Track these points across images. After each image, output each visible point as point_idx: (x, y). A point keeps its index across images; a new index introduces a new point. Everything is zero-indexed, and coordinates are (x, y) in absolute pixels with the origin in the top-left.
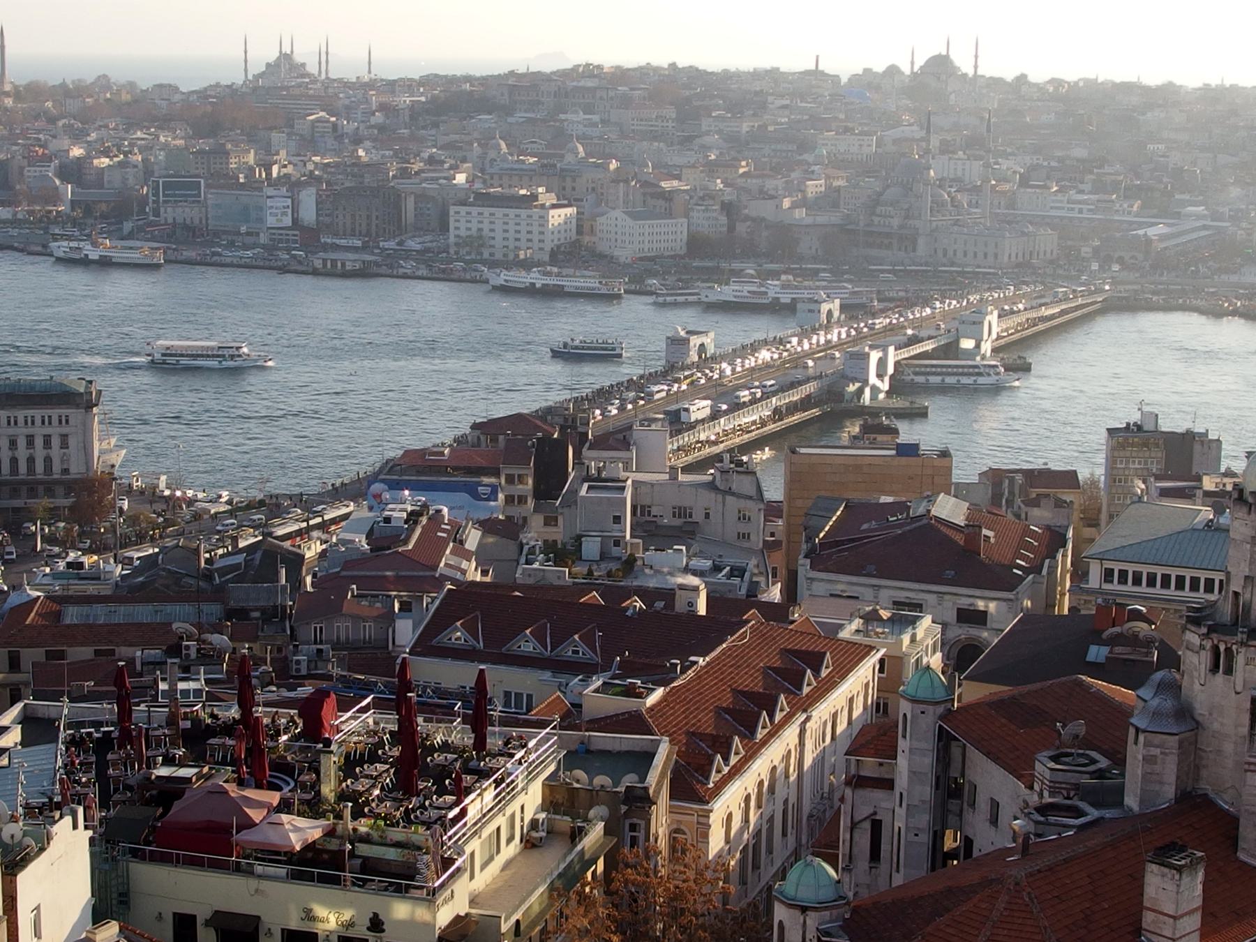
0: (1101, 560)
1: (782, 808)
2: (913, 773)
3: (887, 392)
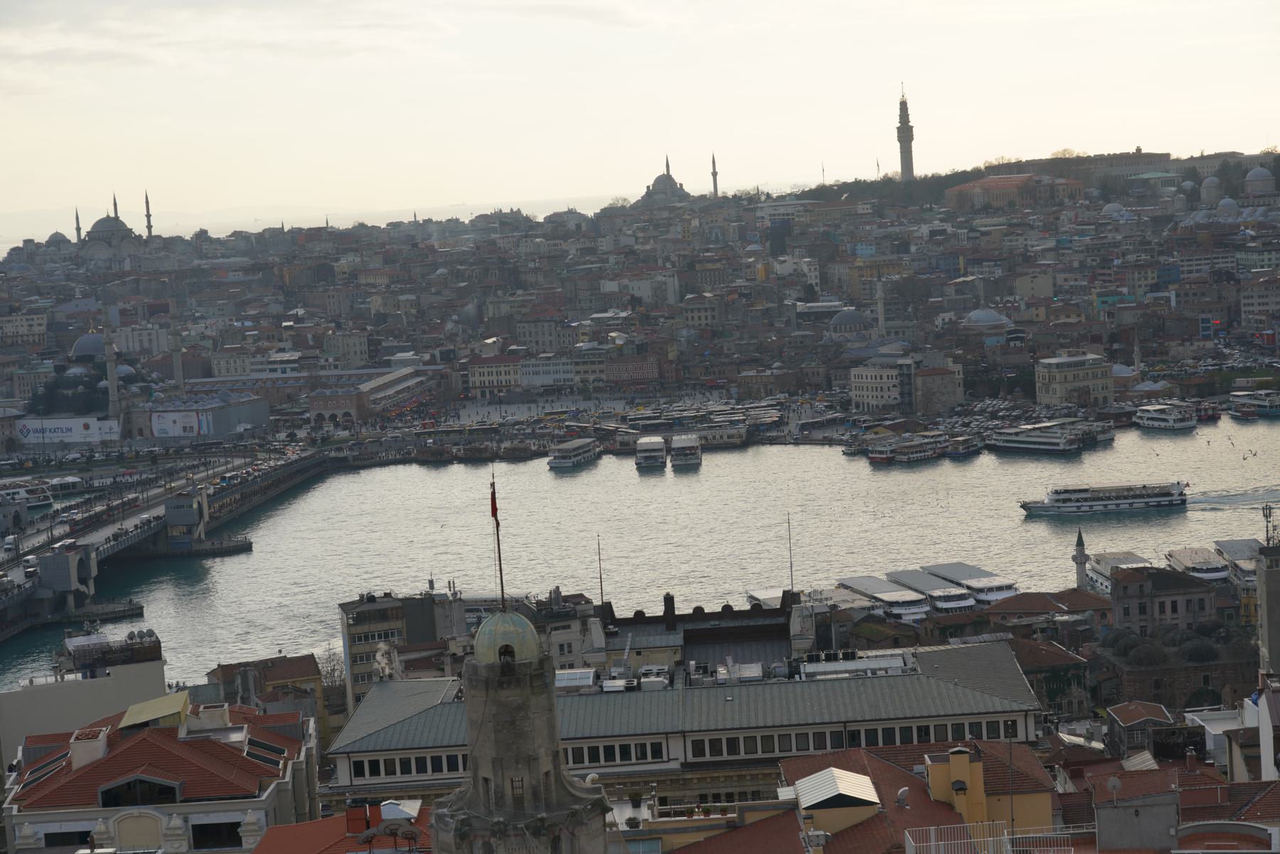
0: (348, 753)
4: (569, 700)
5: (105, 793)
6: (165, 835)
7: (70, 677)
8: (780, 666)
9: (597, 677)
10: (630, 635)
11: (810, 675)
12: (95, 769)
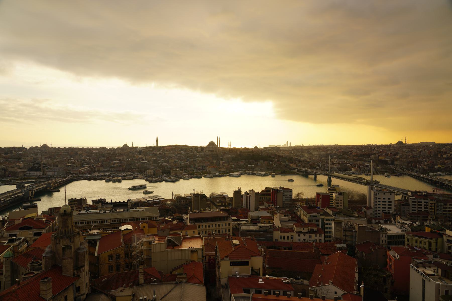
2: (6, 271)
3: (33, 197)
6: (29, 234)
8: (126, 210)
9: (100, 211)
10: (105, 205)
11: (130, 211)
12: (19, 224)
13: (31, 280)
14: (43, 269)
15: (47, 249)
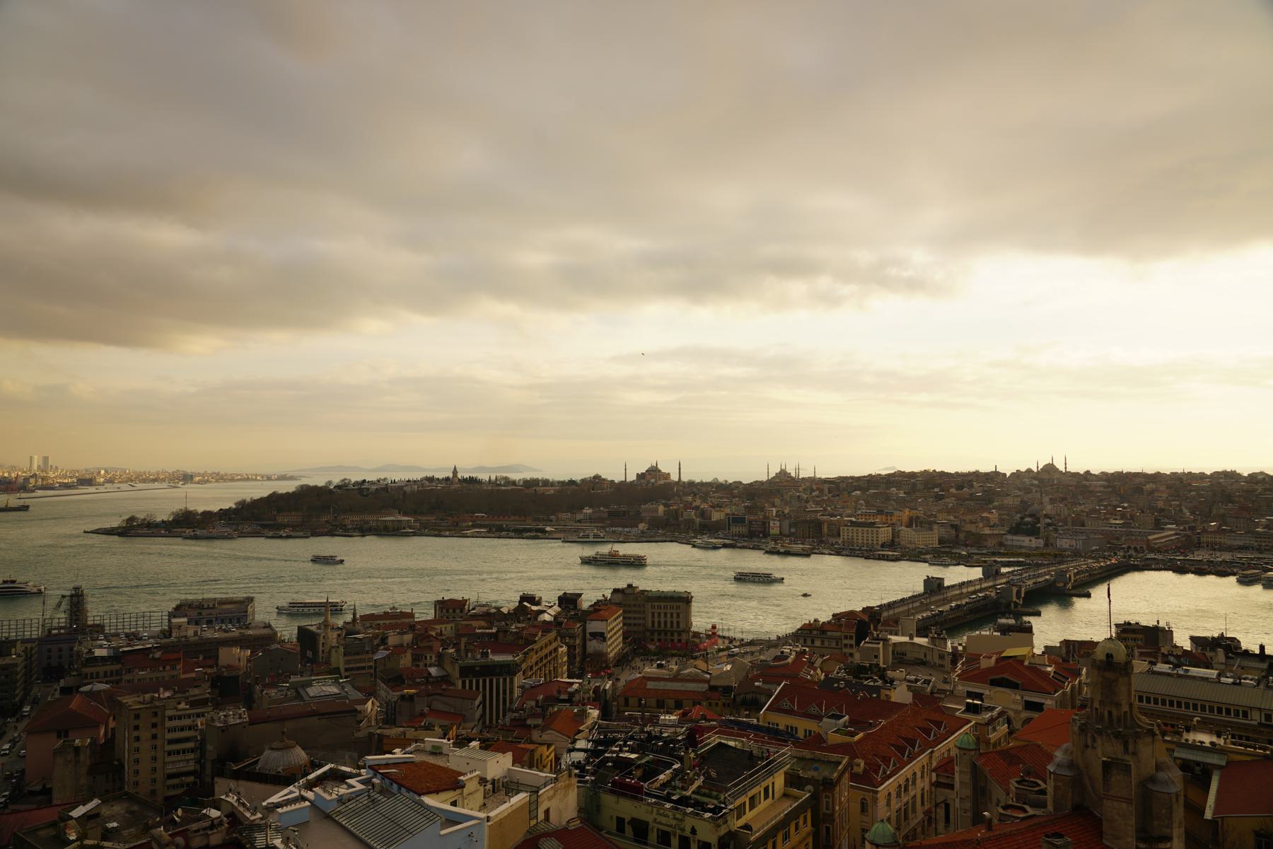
1: (921, 792)
4: (1202, 683)
5: (991, 680)
7: (995, 634)
9: (1219, 675)
10: (1239, 660)
12: (990, 670)
13: (1019, 828)
14: (1050, 807)
15: (1059, 755)
